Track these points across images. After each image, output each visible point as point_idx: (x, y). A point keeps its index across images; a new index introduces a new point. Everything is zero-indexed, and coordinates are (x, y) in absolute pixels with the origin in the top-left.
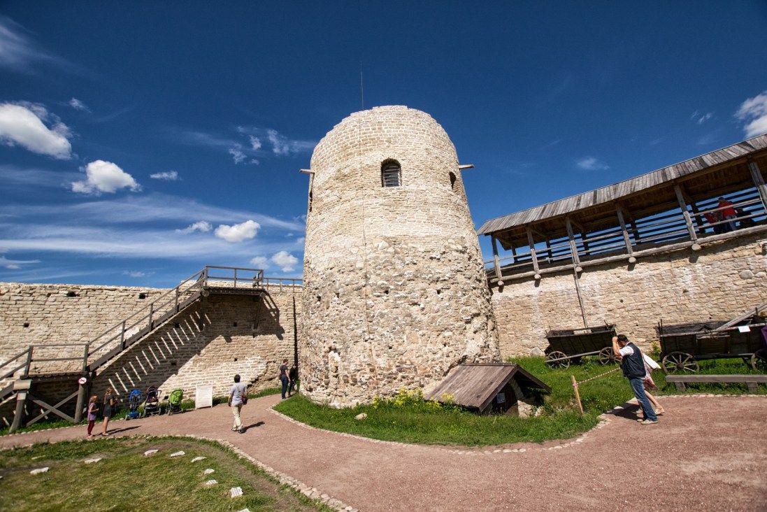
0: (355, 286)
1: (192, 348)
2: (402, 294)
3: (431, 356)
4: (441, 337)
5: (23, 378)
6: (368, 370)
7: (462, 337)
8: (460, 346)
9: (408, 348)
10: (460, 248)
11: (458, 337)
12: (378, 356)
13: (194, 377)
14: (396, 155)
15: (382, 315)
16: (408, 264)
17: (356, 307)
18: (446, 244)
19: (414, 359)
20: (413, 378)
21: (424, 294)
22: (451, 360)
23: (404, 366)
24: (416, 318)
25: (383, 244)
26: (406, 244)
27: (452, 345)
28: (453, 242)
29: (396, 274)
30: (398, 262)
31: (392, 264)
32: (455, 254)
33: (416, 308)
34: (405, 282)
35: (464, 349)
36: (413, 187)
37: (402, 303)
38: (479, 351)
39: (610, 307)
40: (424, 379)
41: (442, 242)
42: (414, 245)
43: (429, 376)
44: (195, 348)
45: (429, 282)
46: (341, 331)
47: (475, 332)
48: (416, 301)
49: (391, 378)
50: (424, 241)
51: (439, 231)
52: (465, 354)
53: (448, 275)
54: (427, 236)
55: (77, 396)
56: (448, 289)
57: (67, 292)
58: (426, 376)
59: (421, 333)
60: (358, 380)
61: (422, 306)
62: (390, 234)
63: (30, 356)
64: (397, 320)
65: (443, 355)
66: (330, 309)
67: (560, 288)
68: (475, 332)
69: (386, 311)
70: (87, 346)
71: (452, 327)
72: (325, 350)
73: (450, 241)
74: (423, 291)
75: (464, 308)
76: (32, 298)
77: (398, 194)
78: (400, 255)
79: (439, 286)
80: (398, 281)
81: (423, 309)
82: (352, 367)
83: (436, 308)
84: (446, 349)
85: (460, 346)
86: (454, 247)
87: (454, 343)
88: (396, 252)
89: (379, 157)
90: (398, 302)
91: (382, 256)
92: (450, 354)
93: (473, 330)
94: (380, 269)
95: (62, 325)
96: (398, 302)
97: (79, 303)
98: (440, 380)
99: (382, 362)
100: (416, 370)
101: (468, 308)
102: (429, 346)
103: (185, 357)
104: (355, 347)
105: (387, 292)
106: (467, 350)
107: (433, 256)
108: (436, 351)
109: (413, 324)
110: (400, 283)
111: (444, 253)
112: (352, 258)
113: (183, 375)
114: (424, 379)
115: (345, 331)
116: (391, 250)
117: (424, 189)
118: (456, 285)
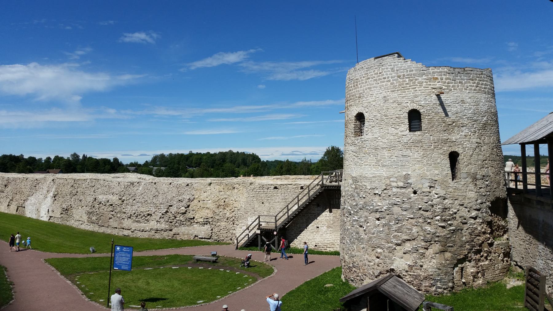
1: (326, 220)
2: (356, 218)
3: (367, 263)
4: (375, 251)
5: (258, 229)
7: (391, 255)
8: (388, 261)
9: (357, 254)
10: (401, 184)
13: (328, 236)
14: (363, 109)
15: (348, 229)
16: (361, 197)
18: (388, 182)
19: (359, 261)
21: (366, 221)
22: (380, 269)
23: (355, 264)
24: (361, 236)
25: (351, 181)
26: (361, 183)
27: (382, 259)
28: (395, 180)
29: (355, 204)
30: (356, 195)
32: (395, 190)
33: (361, 229)
34: (358, 210)
35: (393, 263)
37: (355, 224)
38: (407, 268)
41: (384, 181)
42: (365, 184)
43: (365, 275)
44: (327, 220)
47: (404, 253)
48: (361, 224)
50: (371, 181)
51: (383, 172)
52: (392, 267)
53: (385, 208)
54: (374, 177)
55: (275, 240)
56: (385, 218)
57: (273, 187)
58: (364, 275)
59: (362, 246)
61: (365, 228)
62: (353, 175)
63: (259, 220)
64: (352, 235)
65: (375, 264)
69: (349, 227)
70: (276, 217)
71: (382, 246)
73: (391, 179)
74: (366, 218)
75: (396, 234)
76: (263, 190)
77: (361, 143)
78: (358, 190)
79: (378, 215)
80: (355, 209)
81: (365, 230)
83: (372, 231)
85: (388, 261)
86: (394, 184)
88: (356, 188)
89: (354, 112)
90: (354, 223)
93: (403, 251)
94: (349, 199)
95: (273, 203)
96: (354, 223)
97: (278, 192)
98: (372, 279)
101: (399, 234)
102: (367, 256)
103: (322, 225)
105: (350, 214)
106: (394, 265)
107: (377, 192)
108: (370, 260)
109: (359, 239)
110: (355, 211)
111: (385, 189)
113: (323, 235)
116: (354, 186)
117: (377, 137)
118: (391, 215)
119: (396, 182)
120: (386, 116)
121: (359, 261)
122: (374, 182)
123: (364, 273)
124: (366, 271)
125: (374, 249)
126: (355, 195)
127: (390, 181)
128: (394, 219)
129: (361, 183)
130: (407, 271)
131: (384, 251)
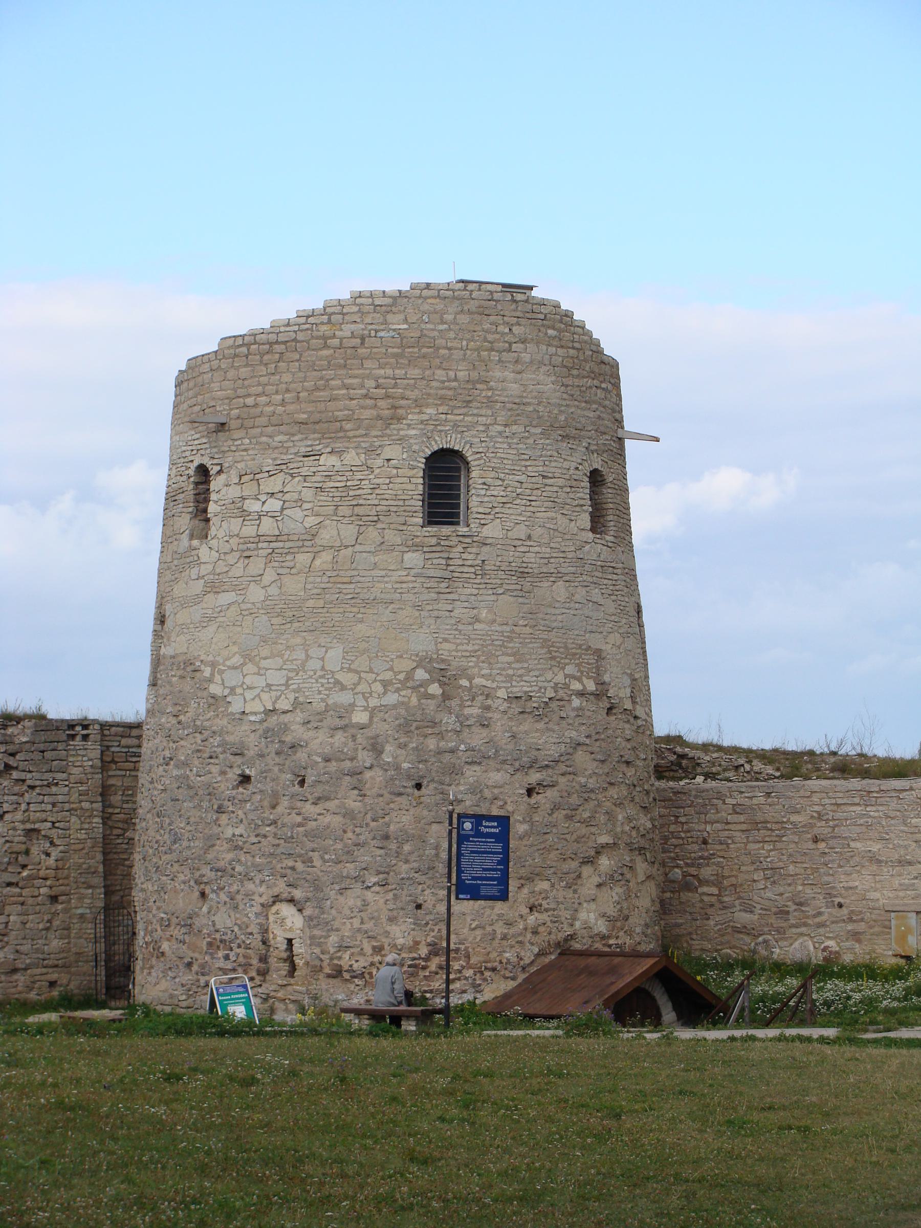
0: (347, 764)
4: (525, 890)
6: (368, 950)
10: (591, 686)
11: (561, 894)
12: (392, 920)
17: (349, 814)
20: (460, 971)
27: (547, 910)
32: (576, 702)
40: (482, 973)
43: (494, 970)
45: (511, 771)
50: (510, 672)
56: (553, 786)
60: (346, 967)
65: (526, 929)
66: (280, 809)
68: (599, 886)
72: (262, 900)
84: (532, 919)
86: (576, 686)
87: (552, 906)
92: (541, 929)
93: (596, 880)
100: (468, 957)
104: (341, 899)
112: (344, 698)
114: (482, 973)
119: (579, 680)
120: (544, 477)
121: (466, 931)
122: (519, 676)
123: (489, 965)
124: (494, 955)
125: (522, 881)
126: (441, 721)
127: (566, 676)
128: (577, 787)
129: (470, 679)
130: (603, 937)
131: (553, 886)
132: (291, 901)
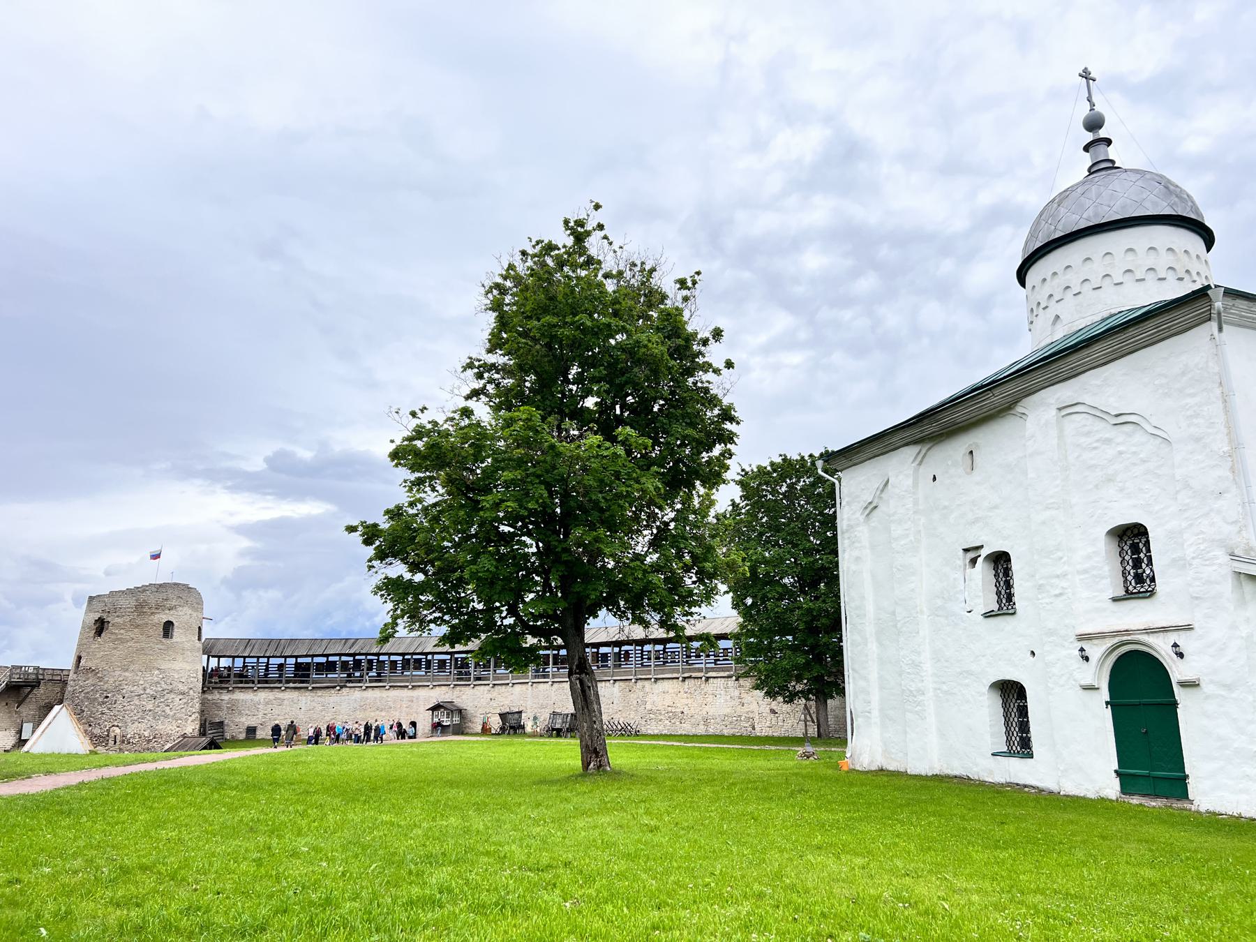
2: (162, 700)
3: (170, 732)
15: (150, 711)
31: (160, 684)
36: (178, 640)
39: (266, 712)
46: (124, 717)
49: (149, 741)
67: (242, 698)
79: (181, 697)
82: (129, 736)
89: (164, 617)
91: (156, 679)
99: (146, 734)
115: (127, 717)
132: (118, 726)
